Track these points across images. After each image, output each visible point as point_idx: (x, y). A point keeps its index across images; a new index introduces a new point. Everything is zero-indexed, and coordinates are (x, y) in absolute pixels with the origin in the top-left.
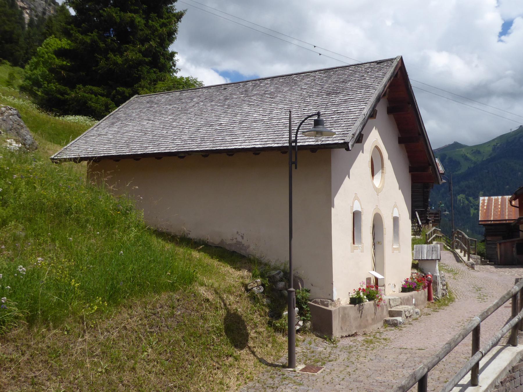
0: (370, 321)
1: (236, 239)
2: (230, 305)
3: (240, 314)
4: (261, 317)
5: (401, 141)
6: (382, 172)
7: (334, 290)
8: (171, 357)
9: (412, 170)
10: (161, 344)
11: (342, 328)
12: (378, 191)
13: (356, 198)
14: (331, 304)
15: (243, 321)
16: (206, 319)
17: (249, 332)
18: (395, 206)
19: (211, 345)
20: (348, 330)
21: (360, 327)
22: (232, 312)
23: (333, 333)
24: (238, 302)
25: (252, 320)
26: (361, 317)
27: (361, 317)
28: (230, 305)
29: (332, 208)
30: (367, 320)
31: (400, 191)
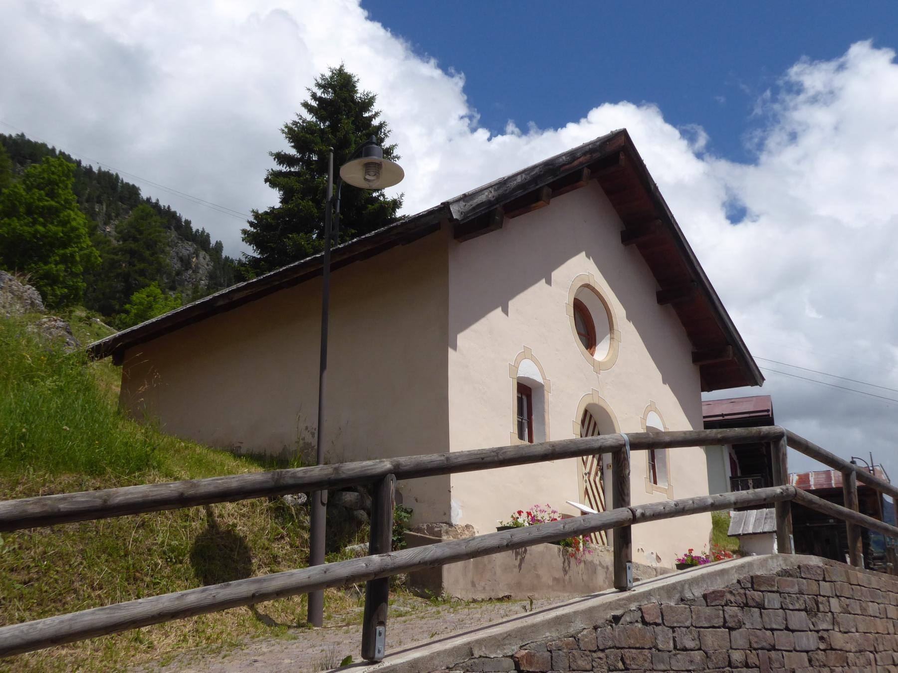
0: (546, 579)
1: (304, 439)
2: (221, 516)
3: (242, 534)
4: (291, 547)
5: (661, 299)
6: (612, 338)
7: (454, 503)
8: (38, 580)
9: (696, 358)
10: (25, 554)
11: (473, 584)
12: (598, 367)
13: (527, 354)
14: (447, 533)
15: (246, 547)
16: (152, 531)
17: (255, 567)
18: (652, 407)
19: (146, 575)
20: (487, 588)
21: (519, 585)
22: (223, 528)
23: (445, 584)
24: (243, 515)
25: (267, 549)
26: (520, 566)
27: (520, 566)
28: (221, 516)
29: (450, 351)
30: (538, 576)
31: (667, 387)
